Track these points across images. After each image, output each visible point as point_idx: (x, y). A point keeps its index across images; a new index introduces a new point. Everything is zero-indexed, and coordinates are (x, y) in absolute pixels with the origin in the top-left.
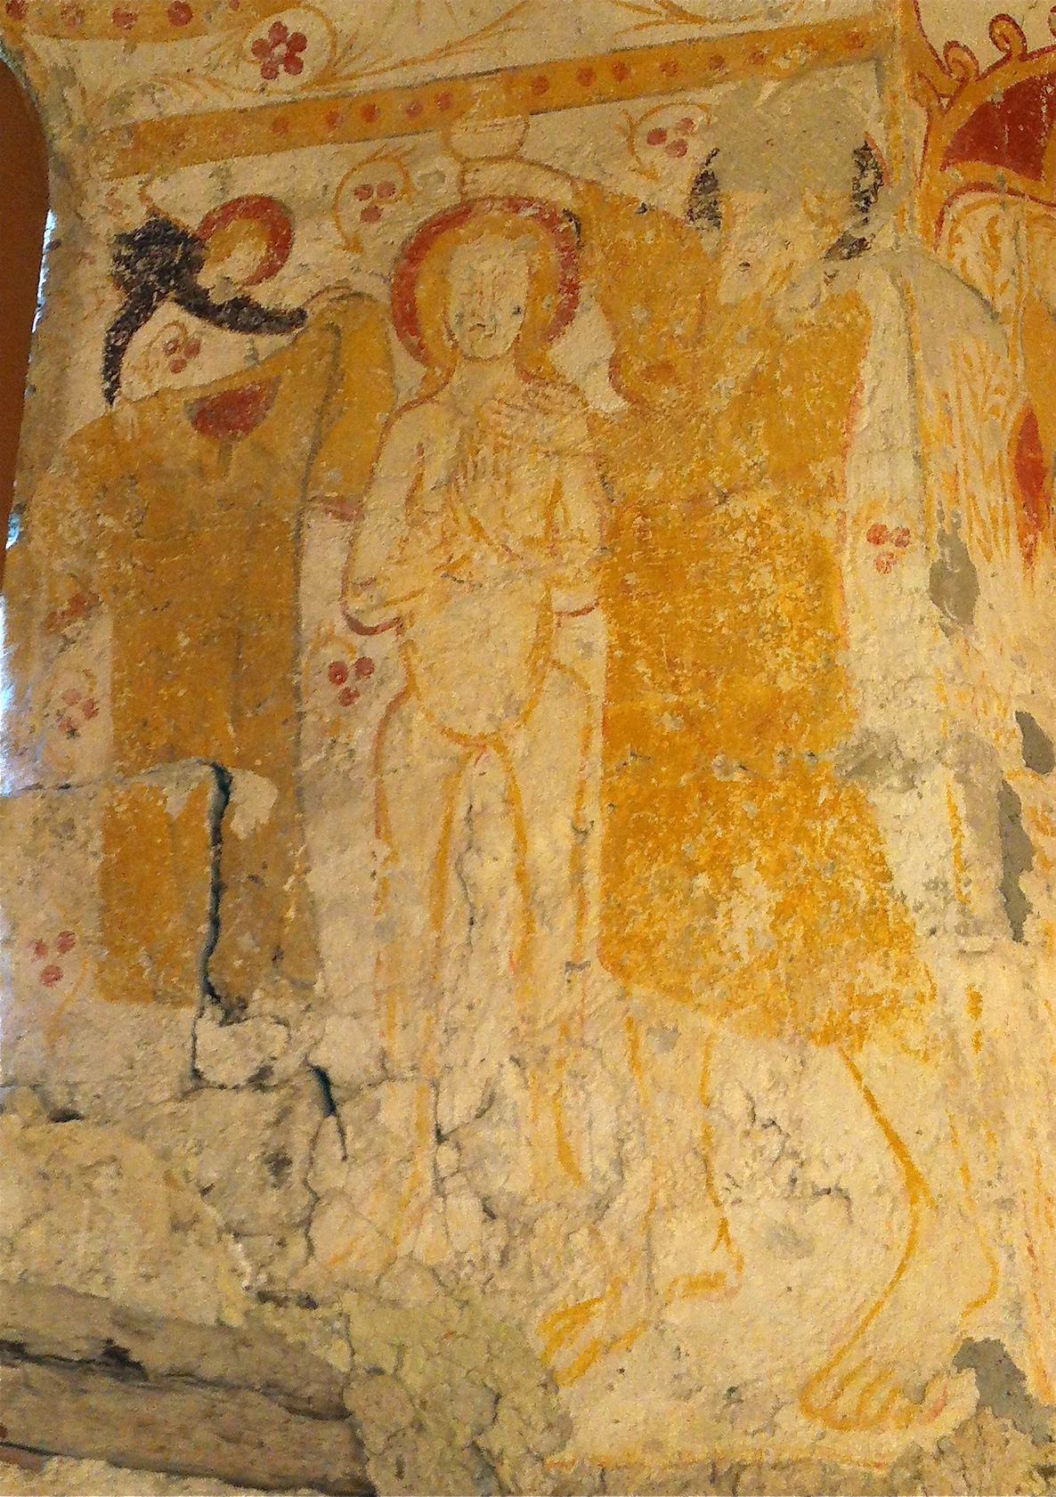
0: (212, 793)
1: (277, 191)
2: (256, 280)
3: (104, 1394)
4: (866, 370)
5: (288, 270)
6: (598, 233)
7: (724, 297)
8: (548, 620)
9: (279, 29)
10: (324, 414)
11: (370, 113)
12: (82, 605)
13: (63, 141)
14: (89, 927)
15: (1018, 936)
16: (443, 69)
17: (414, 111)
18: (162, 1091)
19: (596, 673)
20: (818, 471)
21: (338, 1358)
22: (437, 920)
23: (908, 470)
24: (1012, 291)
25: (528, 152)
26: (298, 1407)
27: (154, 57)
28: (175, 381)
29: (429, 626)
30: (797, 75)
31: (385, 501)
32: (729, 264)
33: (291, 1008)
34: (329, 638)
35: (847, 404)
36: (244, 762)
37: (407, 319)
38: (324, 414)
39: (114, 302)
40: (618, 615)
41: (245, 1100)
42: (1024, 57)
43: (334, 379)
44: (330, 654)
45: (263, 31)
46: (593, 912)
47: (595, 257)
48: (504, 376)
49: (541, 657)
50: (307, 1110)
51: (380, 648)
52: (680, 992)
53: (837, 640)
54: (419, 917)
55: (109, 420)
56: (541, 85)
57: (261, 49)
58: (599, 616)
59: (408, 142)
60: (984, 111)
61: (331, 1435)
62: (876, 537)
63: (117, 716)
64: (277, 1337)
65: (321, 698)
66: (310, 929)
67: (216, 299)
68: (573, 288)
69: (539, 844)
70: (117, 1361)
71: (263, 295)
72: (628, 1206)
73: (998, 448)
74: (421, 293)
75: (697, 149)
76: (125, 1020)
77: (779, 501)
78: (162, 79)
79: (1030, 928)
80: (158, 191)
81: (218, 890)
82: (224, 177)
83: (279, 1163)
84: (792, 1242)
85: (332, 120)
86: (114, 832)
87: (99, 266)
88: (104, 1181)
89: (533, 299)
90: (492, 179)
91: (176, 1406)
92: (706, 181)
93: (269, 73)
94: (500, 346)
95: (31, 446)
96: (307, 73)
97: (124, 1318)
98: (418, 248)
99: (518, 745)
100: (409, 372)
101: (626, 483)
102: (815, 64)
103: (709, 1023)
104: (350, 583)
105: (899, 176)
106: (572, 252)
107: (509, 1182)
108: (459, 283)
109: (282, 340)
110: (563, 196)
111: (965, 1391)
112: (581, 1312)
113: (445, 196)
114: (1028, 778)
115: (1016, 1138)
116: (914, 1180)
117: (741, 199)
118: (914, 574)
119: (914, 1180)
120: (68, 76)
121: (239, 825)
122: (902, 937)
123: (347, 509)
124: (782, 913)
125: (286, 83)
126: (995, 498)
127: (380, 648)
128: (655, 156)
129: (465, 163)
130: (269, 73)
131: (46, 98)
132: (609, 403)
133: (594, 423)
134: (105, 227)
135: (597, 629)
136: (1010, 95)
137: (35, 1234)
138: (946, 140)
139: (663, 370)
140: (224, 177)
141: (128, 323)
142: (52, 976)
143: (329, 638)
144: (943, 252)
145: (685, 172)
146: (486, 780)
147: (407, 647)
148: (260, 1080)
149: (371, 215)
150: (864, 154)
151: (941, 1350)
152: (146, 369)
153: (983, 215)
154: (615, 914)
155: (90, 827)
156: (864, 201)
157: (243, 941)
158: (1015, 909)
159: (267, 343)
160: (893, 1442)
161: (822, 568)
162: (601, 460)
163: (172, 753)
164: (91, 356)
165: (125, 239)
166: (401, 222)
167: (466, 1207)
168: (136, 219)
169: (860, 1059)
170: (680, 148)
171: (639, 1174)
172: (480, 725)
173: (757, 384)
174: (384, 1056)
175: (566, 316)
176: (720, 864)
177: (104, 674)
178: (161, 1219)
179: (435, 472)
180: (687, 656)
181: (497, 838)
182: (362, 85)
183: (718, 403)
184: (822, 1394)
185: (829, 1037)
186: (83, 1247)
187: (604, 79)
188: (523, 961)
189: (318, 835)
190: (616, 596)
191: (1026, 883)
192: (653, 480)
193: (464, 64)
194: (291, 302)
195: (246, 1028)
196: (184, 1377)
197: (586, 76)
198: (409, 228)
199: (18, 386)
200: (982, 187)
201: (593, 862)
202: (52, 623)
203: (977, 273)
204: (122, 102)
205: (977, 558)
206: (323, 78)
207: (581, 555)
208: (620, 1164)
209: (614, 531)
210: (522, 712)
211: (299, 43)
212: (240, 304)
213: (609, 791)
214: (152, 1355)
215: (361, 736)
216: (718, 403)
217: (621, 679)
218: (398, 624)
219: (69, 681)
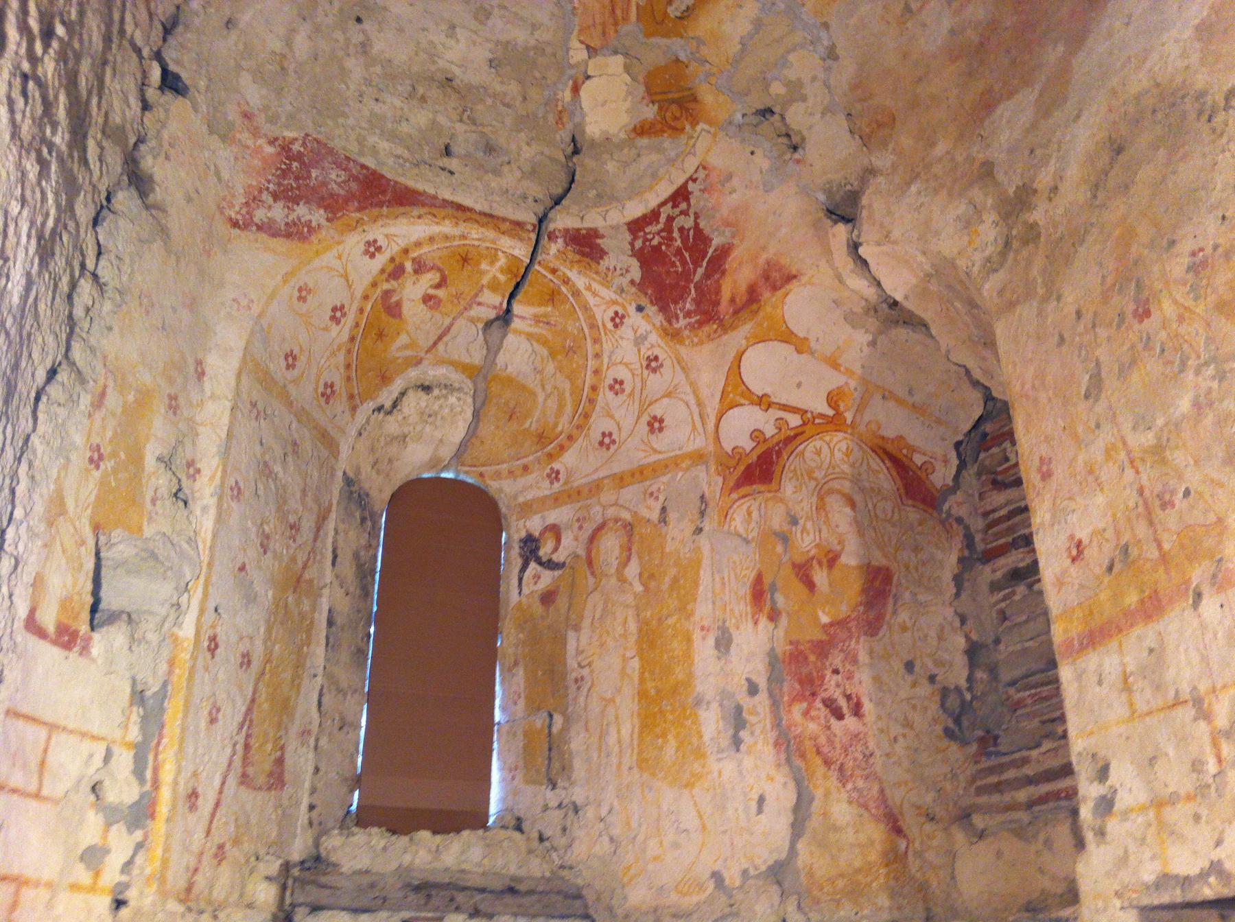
0: (548, 720)
1: (557, 522)
2: (553, 552)
3: (508, 899)
4: (702, 572)
5: (561, 549)
6: (636, 530)
7: (667, 550)
8: (625, 660)
9: (552, 469)
10: (571, 597)
11: (579, 493)
12: (516, 664)
13: (504, 510)
14: (521, 764)
15: (738, 750)
16: (595, 477)
17: (590, 491)
18: (539, 809)
19: (636, 675)
20: (689, 607)
21: (580, 882)
22: (599, 756)
23: (710, 606)
24: (756, 530)
25: (621, 502)
26: (567, 896)
27: (522, 481)
28: (535, 588)
29: (598, 664)
30: (687, 469)
31: (586, 623)
32: (669, 538)
33: (566, 784)
34: (573, 670)
35: (696, 584)
36: (555, 710)
37: (590, 563)
38: (571, 597)
39: (519, 562)
40: (641, 659)
41: (557, 812)
42: (765, 440)
43: (573, 585)
44: (574, 675)
45: (548, 471)
46: (636, 751)
47: (636, 538)
48: (613, 580)
49: (623, 673)
50: (571, 813)
51: (585, 672)
52: (654, 775)
53: (692, 664)
54: (595, 756)
55: (520, 603)
56: (622, 479)
57: (549, 476)
58: (637, 659)
59: (589, 501)
60: (749, 467)
61: (578, 903)
62: (703, 628)
63: (526, 697)
64: (562, 878)
65: (573, 688)
66: (571, 761)
67: (544, 559)
68: (630, 549)
69: (623, 732)
70: (512, 890)
71: (555, 558)
72: (641, 838)
73: (745, 590)
74: (593, 554)
75: (662, 498)
76: (530, 789)
77: (680, 619)
78: (525, 489)
79: (743, 747)
80: (528, 524)
81: (550, 749)
82: (543, 518)
83: (564, 829)
84: (676, 845)
85: (569, 496)
86: (526, 734)
87: (516, 550)
88: (505, 844)
89: (621, 553)
90: (611, 512)
91: (527, 901)
92: (664, 509)
93: (552, 483)
94: (613, 571)
95: (502, 612)
96: (562, 482)
97: (513, 879)
98: (592, 539)
99: (618, 700)
100: (591, 580)
101: (643, 615)
102: (692, 466)
103: (660, 783)
104: (579, 652)
105: (712, 505)
106: (630, 535)
107: (616, 832)
108: (602, 547)
109: (560, 572)
110: (626, 516)
111: (711, 885)
112: (628, 868)
113: (599, 519)
114: (748, 699)
115: (730, 812)
116: (704, 827)
117: (672, 516)
118: (711, 641)
119: (704, 827)
120: (501, 490)
121: (555, 730)
122: (703, 756)
123: (577, 628)
124: (677, 750)
125: (556, 485)
126: (742, 607)
127: (585, 672)
128: (651, 502)
129: (604, 507)
130: (552, 483)
131: (496, 497)
132: (639, 588)
133: (635, 595)
134: (516, 537)
135: (635, 663)
136: (759, 457)
137: (486, 861)
138: (732, 484)
139: (652, 576)
140: (543, 518)
141: (523, 569)
142: (513, 778)
143: (573, 670)
144: (726, 527)
145: (657, 506)
146: (611, 711)
147: (592, 672)
148: (560, 806)
149: (580, 528)
150: (702, 497)
151: (707, 875)
152: (528, 584)
153: (745, 507)
154: (640, 752)
155: (520, 736)
156: (702, 514)
157: (556, 765)
158: (737, 743)
159: (557, 573)
160: (695, 899)
161: (689, 640)
162: (637, 608)
163: (539, 709)
164: (515, 582)
165: (521, 540)
166: (589, 528)
167: (606, 839)
168: (523, 534)
169: (694, 792)
170: (657, 498)
171: (644, 827)
172: (609, 695)
173: (675, 580)
174: (587, 797)
175: (629, 559)
176: (664, 735)
177: (522, 686)
178: (523, 849)
179: (597, 616)
180: (657, 671)
181: (613, 730)
182: (576, 484)
183: (665, 587)
184: (680, 888)
185: (686, 786)
186: (500, 862)
187: (637, 475)
188: (619, 765)
189: (573, 733)
190: (640, 652)
191: (742, 734)
192: (649, 614)
193: (601, 474)
194: (562, 559)
195: (557, 791)
196: (531, 892)
197: (633, 475)
198: (590, 532)
199: (498, 592)
200: (744, 496)
201: (636, 736)
202: (510, 670)
203: (741, 530)
204: (515, 497)
205: (732, 630)
206: (565, 483)
207: (632, 639)
208: (640, 825)
209: (640, 631)
210: (619, 690)
211: (558, 473)
212: (550, 561)
213: (639, 714)
214: (522, 887)
215: (582, 700)
216: (665, 587)
217: (642, 680)
218: (590, 664)
219: (514, 688)
